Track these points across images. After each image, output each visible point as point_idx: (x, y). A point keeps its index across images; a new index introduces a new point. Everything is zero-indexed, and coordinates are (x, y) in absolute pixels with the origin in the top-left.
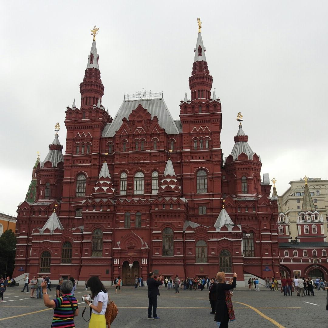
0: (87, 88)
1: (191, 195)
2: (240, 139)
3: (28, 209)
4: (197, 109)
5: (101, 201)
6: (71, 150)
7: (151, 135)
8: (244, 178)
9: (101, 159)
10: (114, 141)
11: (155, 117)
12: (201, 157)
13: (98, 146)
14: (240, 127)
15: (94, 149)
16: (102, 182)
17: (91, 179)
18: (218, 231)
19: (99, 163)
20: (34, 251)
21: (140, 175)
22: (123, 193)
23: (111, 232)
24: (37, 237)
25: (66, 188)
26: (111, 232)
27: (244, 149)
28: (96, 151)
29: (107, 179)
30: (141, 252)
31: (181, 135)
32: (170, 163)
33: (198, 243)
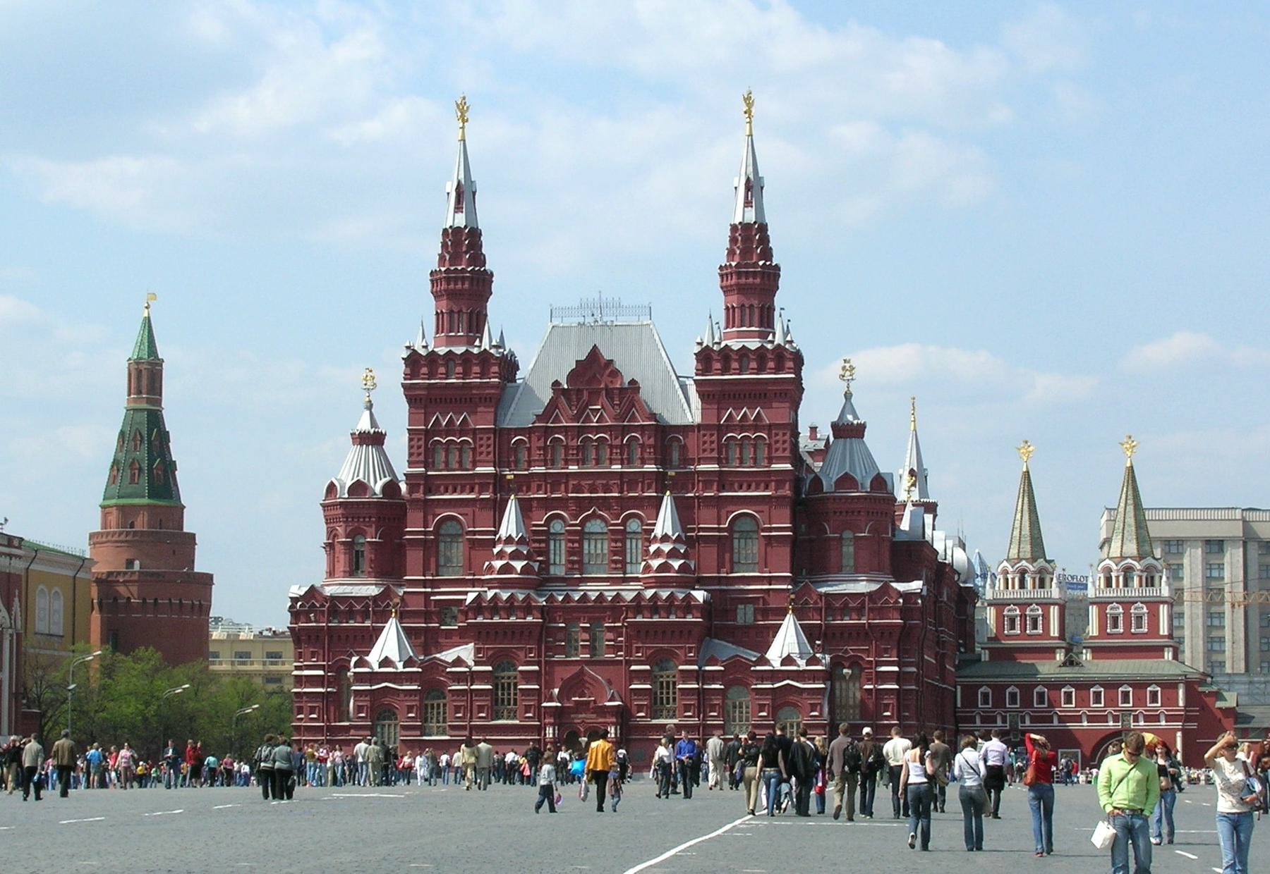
0: (452, 286)
1: (719, 580)
2: (849, 431)
3: (322, 606)
4: (735, 365)
5: (512, 597)
6: (422, 458)
7: (625, 430)
8: (848, 534)
9: (500, 486)
10: (529, 438)
11: (633, 382)
12: (745, 486)
13: (491, 449)
14: (848, 396)
15: (483, 457)
16: (509, 549)
17: (474, 533)
18: (777, 665)
19: (495, 493)
20: (359, 709)
21: (595, 526)
22: (558, 571)
23: (536, 668)
24: (360, 678)
25: (414, 557)
26: (536, 668)
27: (852, 461)
28: (484, 463)
29: (522, 541)
30: (603, 711)
31: (699, 426)
32: (667, 502)
33: (731, 691)
